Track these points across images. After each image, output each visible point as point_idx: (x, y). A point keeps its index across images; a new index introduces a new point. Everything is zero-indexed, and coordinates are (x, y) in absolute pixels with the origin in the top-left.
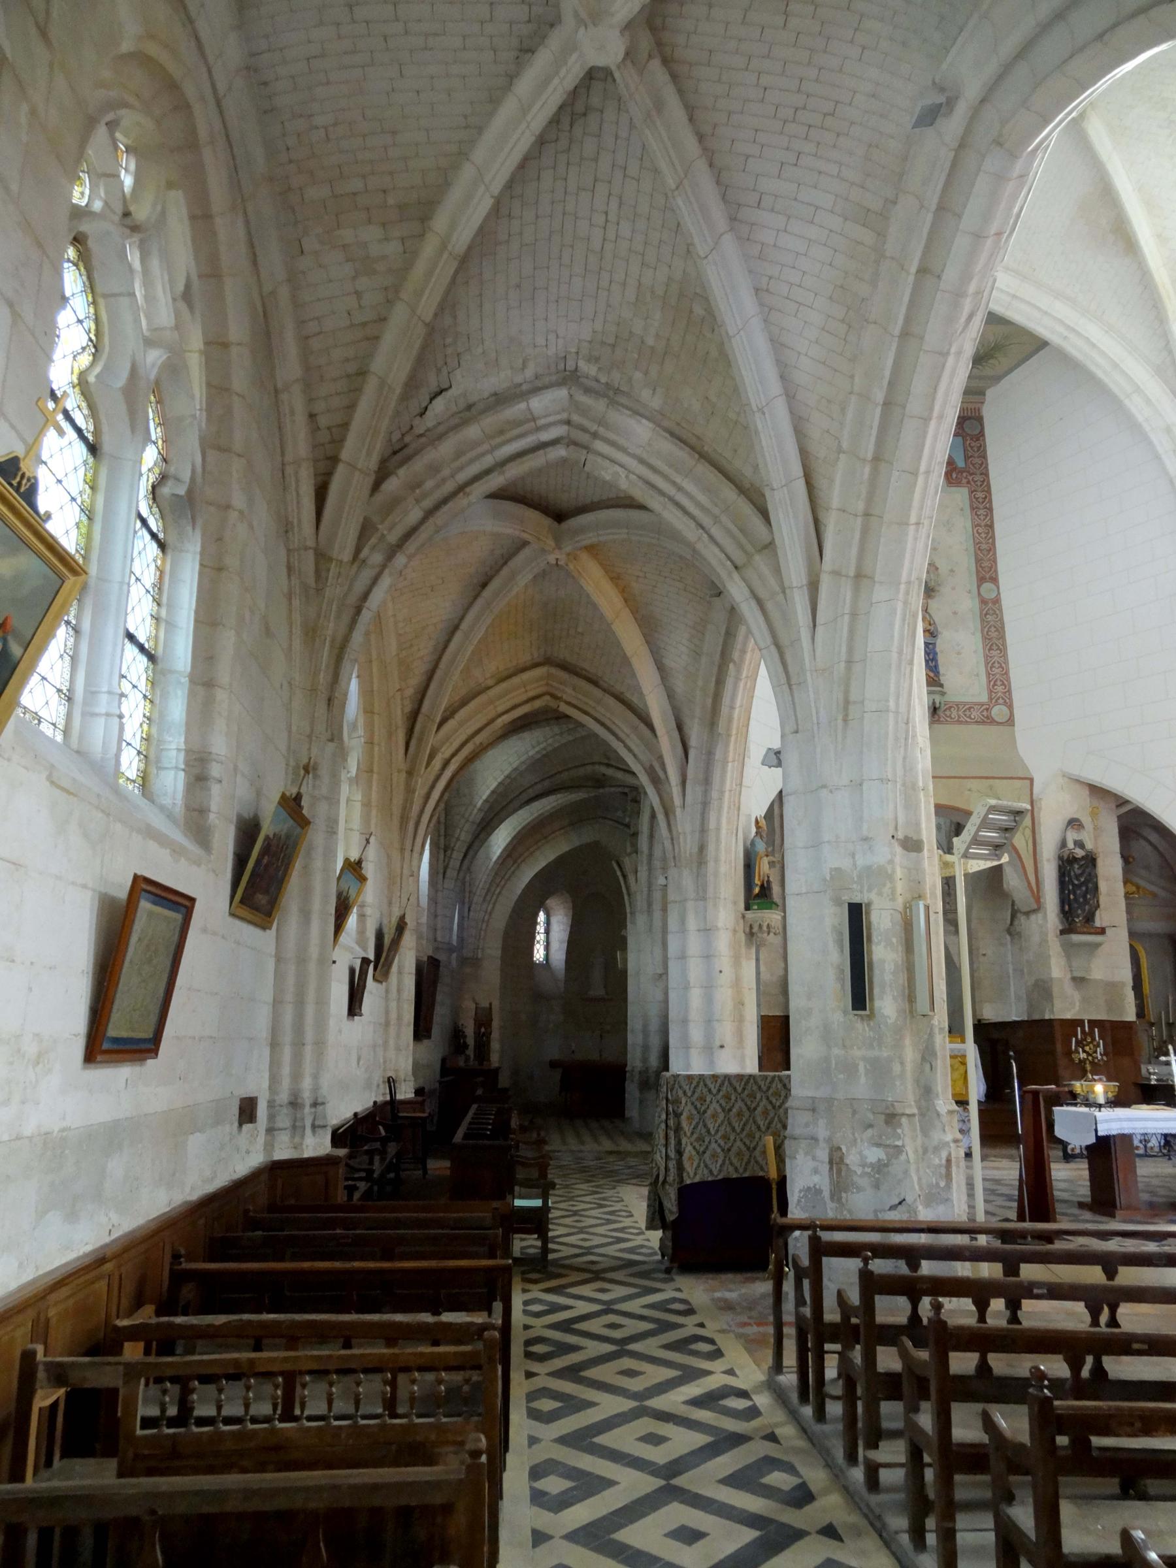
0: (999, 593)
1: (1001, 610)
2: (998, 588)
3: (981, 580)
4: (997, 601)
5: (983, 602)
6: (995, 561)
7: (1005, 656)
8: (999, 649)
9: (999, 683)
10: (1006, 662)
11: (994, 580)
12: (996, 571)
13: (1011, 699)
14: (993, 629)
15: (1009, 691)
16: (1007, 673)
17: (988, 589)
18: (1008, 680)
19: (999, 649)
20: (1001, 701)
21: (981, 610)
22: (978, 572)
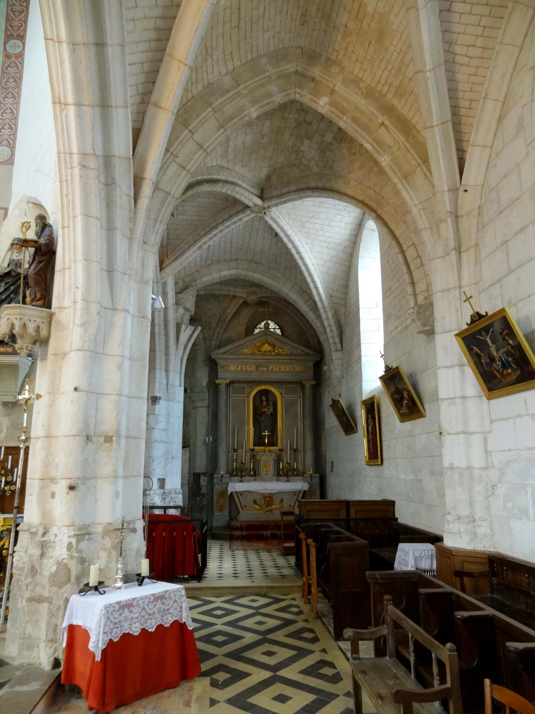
0: (24, 49)
1: (22, 63)
2: (24, 45)
3: (8, 37)
4: (20, 56)
5: (7, 56)
6: (26, 22)
7: (18, 104)
8: (14, 97)
9: (7, 126)
10: (17, 109)
11: (22, 38)
12: (25, 30)
13: (14, 141)
14: (11, 80)
15: (15, 134)
16: (16, 118)
17: (13, 46)
18: (16, 125)
19: (14, 97)
20: (5, 142)
21: (4, 63)
22: (6, 29)
